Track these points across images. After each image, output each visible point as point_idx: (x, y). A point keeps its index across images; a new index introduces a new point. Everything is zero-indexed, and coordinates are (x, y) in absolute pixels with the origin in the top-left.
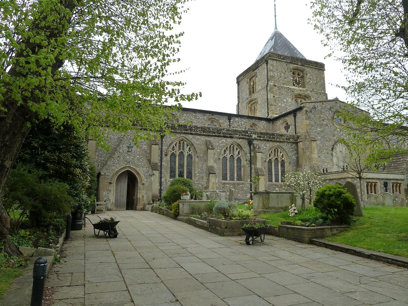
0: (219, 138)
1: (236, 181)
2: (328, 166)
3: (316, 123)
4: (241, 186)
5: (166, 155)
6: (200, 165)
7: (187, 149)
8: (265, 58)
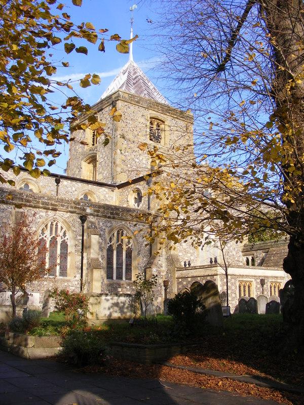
2: (192, 258)
4: (66, 284)
8: (113, 97)
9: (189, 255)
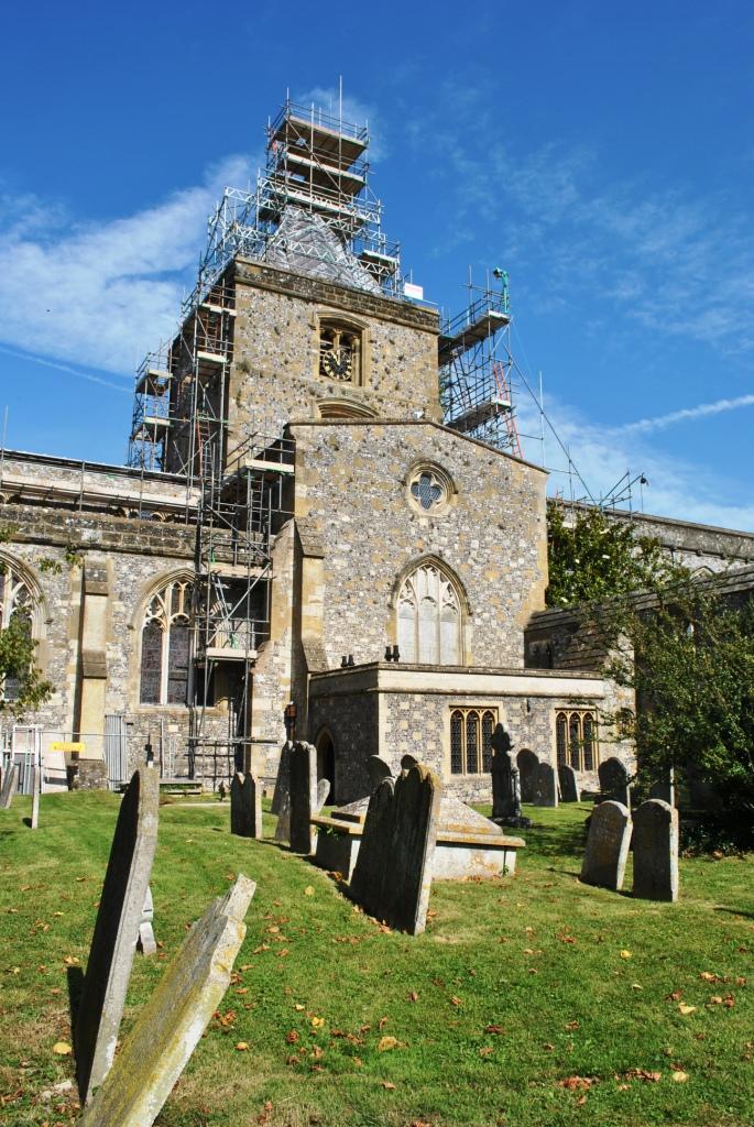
3: (334, 495)
9: (365, 640)
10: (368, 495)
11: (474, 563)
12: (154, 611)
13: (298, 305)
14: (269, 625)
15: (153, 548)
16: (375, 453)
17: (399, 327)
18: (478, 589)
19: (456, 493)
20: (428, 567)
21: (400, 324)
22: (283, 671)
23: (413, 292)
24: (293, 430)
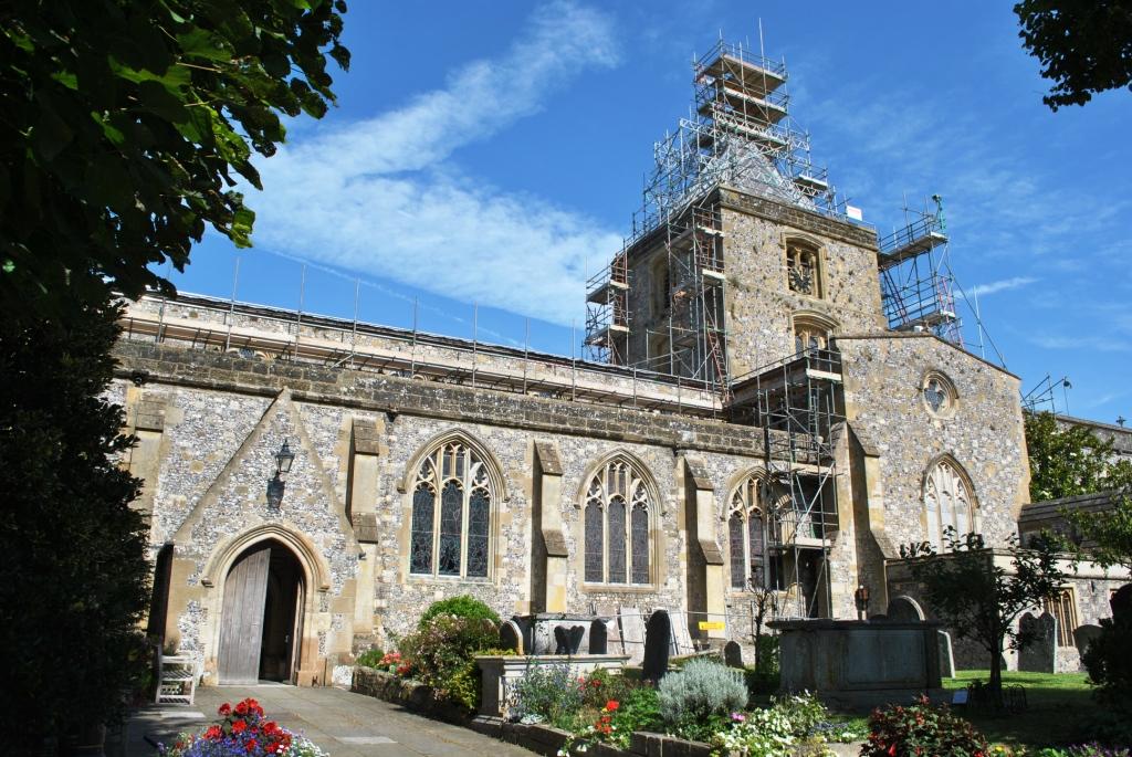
0: (578, 439)
1: (629, 585)
3: (872, 401)
4: (647, 600)
5: (401, 491)
6: (515, 529)
7: (471, 472)
9: (906, 530)
10: (896, 401)
11: (976, 461)
12: (735, 504)
13: (769, 228)
14: (837, 517)
15: (735, 448)
16: (897, 363)
17: (846, 245)
18: (981, 484)
19: (958, 398)
20: (943, 464)
21: (848, 243)
22: (850, 558)
23: (854, 213)
24: (838, 342)
